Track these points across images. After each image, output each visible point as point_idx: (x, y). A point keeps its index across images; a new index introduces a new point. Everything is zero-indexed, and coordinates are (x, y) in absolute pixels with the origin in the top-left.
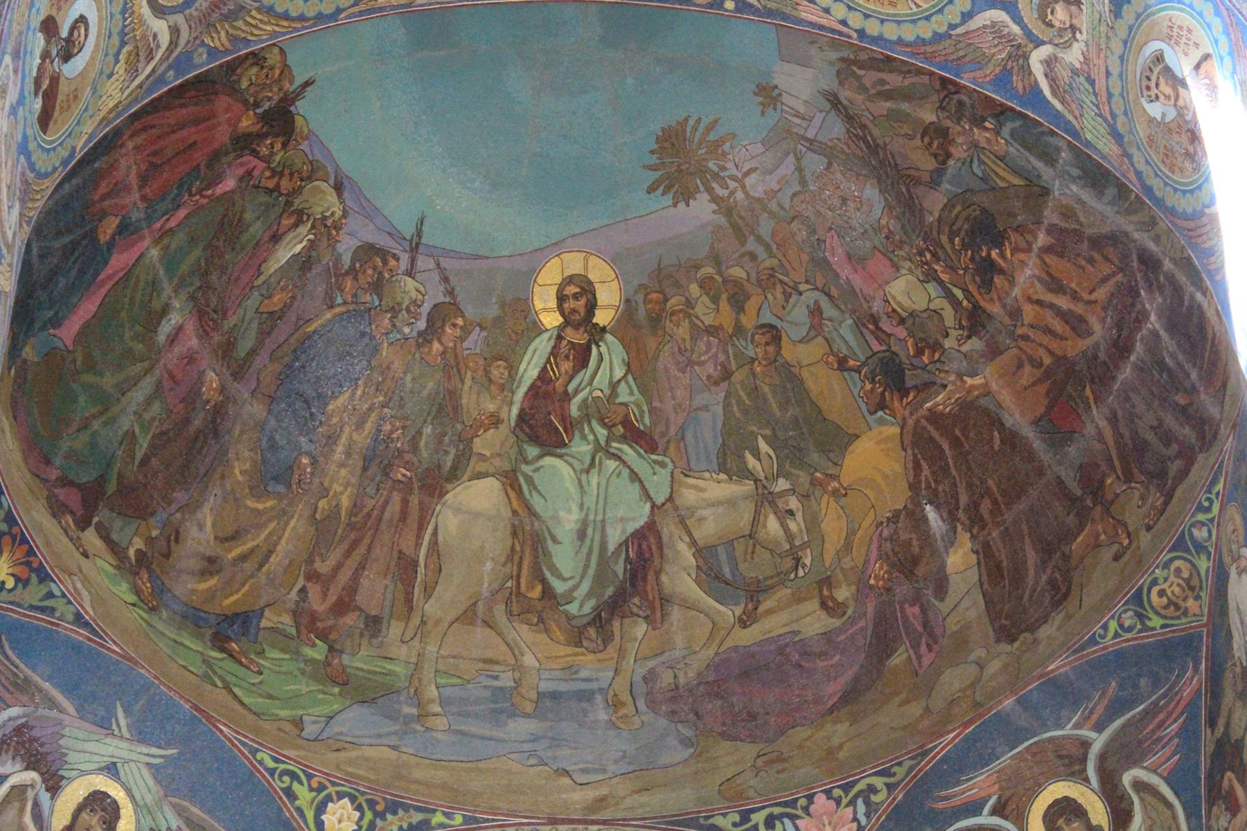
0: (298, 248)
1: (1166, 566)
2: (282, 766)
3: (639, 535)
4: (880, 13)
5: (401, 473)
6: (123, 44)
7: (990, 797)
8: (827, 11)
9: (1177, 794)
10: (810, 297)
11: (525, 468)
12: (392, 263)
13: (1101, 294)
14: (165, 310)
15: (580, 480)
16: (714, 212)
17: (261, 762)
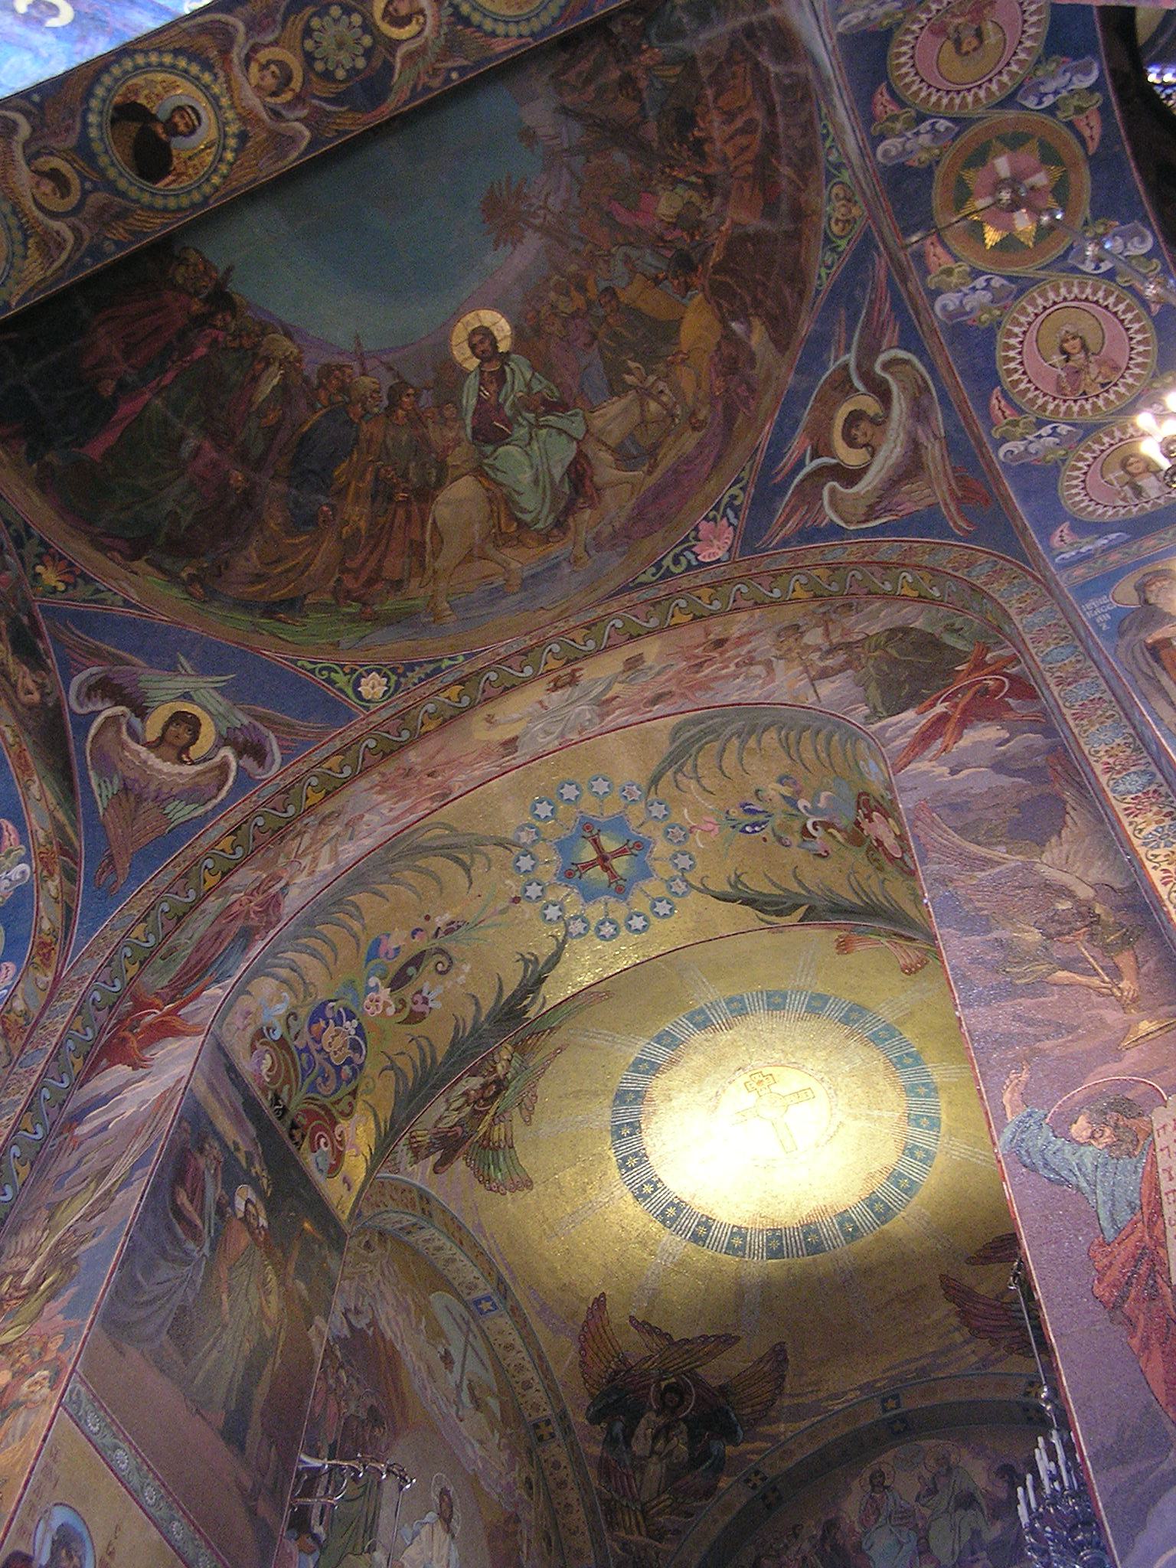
0: (275, 381)
1: (830, 200)
2: (320, 666)
3: (575, 462)
4: (532, 11)
5: (401, 496)
6: (26, 237)
7: (805, 451)
8: (507, 36)
9: (909, 351)
10: (619, 252)
11: (486, 461)
12: (348, 371)
13: (749, 92)
14: (182, 438)
15: (527, 454)
16: (540, 239)
17: (302, 667)
